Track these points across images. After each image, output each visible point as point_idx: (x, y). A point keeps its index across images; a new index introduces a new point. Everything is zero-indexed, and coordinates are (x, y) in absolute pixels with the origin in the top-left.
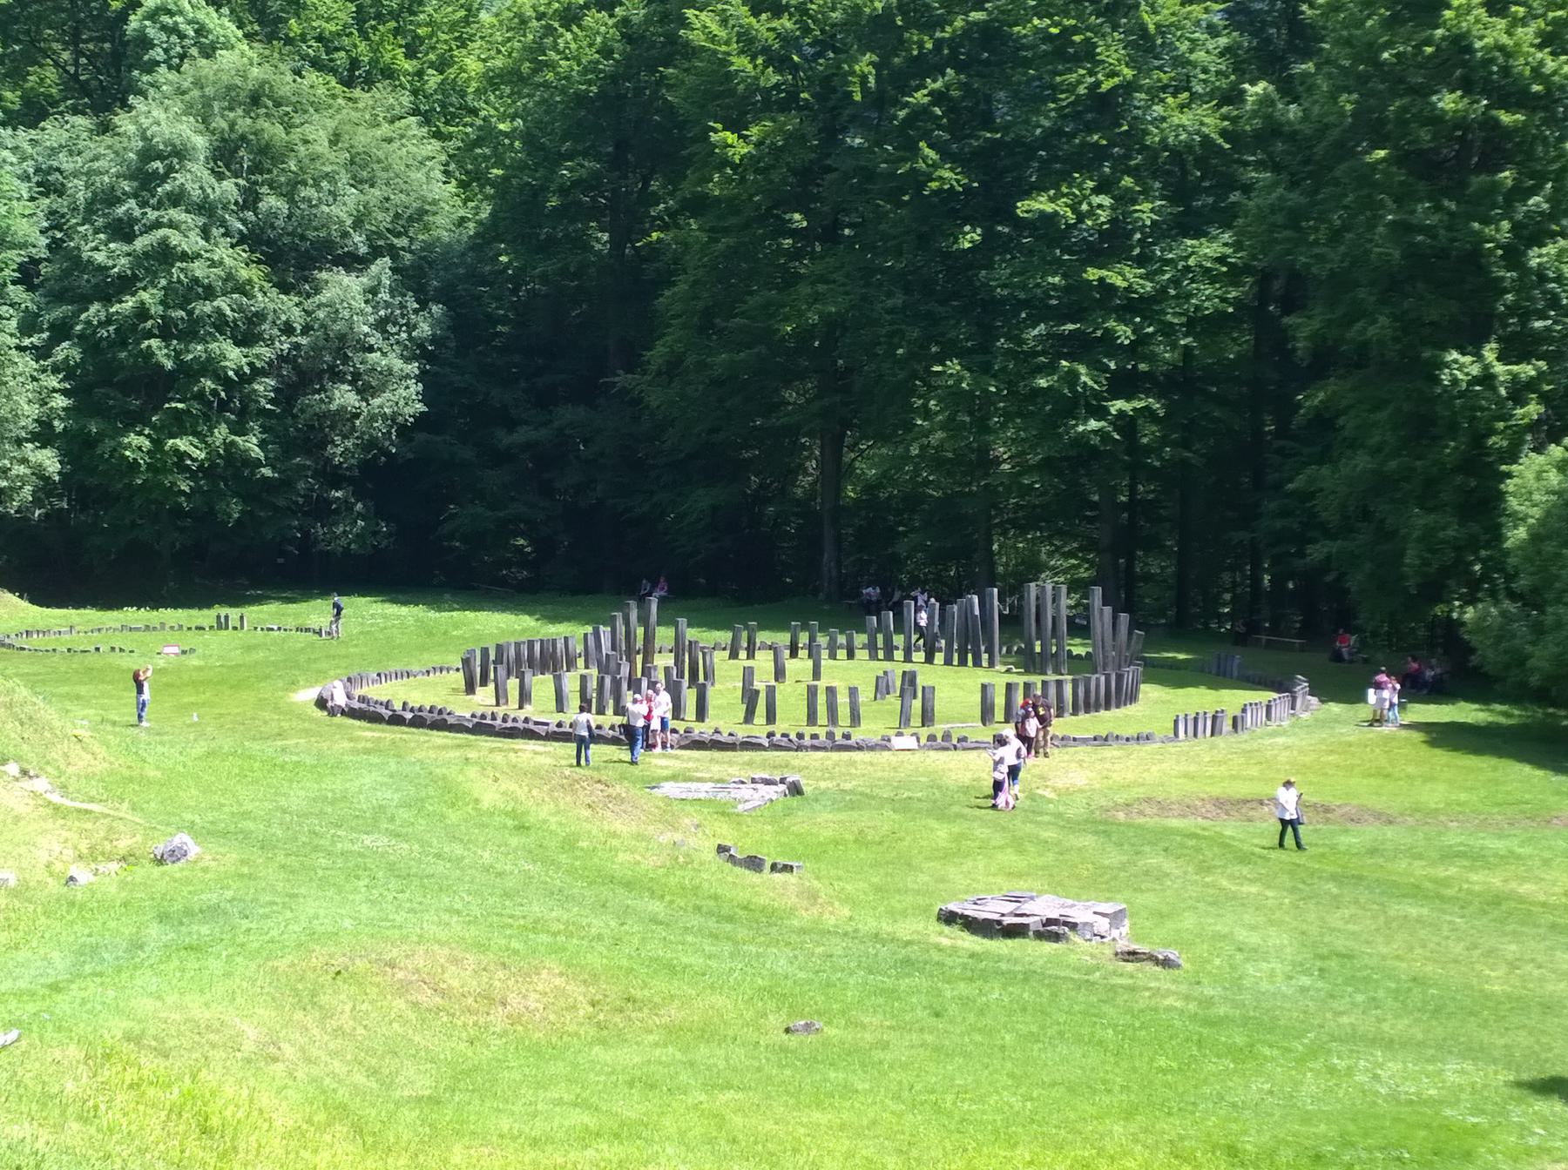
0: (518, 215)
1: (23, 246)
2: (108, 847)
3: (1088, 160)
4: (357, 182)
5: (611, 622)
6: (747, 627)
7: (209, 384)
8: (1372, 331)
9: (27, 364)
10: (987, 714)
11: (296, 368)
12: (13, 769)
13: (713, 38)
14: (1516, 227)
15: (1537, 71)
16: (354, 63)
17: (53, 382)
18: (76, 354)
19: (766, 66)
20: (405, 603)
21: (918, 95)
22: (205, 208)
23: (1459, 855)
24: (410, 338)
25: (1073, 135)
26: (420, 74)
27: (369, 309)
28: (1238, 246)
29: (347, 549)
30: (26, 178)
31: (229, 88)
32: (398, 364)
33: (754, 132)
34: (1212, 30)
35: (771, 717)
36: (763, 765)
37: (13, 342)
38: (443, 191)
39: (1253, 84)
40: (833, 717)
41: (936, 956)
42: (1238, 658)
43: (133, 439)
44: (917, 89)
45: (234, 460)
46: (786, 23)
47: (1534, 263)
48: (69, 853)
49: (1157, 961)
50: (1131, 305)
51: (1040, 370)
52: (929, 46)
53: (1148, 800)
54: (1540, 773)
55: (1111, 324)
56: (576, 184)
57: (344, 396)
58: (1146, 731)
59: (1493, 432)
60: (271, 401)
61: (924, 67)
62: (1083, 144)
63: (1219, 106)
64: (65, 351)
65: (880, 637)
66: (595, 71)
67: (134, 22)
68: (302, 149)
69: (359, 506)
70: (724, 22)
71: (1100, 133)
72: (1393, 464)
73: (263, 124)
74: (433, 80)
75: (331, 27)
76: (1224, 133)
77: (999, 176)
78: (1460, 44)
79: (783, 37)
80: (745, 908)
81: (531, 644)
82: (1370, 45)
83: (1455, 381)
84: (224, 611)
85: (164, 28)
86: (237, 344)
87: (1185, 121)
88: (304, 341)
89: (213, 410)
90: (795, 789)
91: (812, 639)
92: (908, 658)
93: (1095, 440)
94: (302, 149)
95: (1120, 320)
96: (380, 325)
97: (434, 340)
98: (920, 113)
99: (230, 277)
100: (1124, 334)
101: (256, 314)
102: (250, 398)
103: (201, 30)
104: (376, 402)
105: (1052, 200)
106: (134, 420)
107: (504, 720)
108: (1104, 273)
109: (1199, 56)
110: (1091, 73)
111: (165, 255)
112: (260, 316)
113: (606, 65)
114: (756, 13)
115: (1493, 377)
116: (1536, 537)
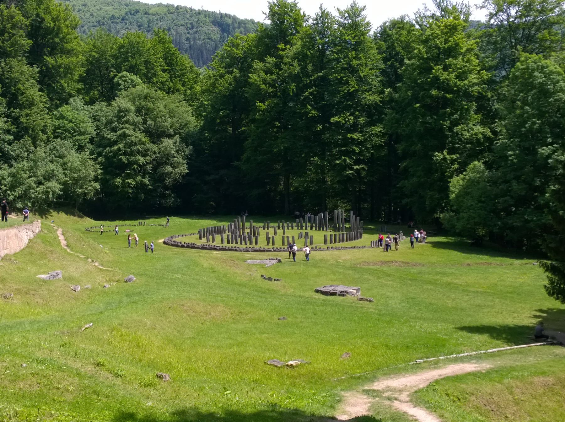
0: (210, 124)
1: (90, 134)
2: (113, 278)
3: (347, 108)
4: (171, 117)
5: (234, 222)
7: (136, 166)
8: (416, 148)
9: (91, 162)
10: (325, 242)
12: (90, 260)
13: (256, 81)
14: (451, 122)
15: (455, 85)
17: (98, 167)
18: (103, 160)
19: (269, 87)
20: (184, 218)
22: (134, 124)
23: (440, 273)
25: (343, 102)
26: (185, 90)
28: (384, 128)
30: (91, 117)
31: (139, 95)
32: (181, 161)
33: (267, 103)
34: (377, 76)
35: (273, 244)
36: (272, 255)
38: (192, 119)
41: (314, 300)
43: (118, 180)
45: (142, 184)
46: (274, 77)
47: (455, 131)
48: (104, 280)
49: (368, 301)
50: (359, 143)
51: (337, 159)
52: (309, 81)
53: (365, 262)
54: (459, 253)
55: (354, 147)
56: (224, 116)
57: (169, 169)
58: (364, 245)
59: (447, 172)
61: (308, 86)
62: (346, 104)
64: (101, 159)
65: (299, 224)
67: (116, 79)
70: (259, 77)
72: (422, 180)
74: (189, 92)
76: (380, 101)
77: (326, 112)
78: (437, 78)
81: (215, 227)
82: (415, 79)
83: (437, 159)
84: (140, 221)
85: (123, 81)
86: (142, 157)
87: (372, 98)
88: (159, 155)
89: (137, 173)
90: (280, 261)
91: (283, 225)
92: (306, 229)
95: (356, 146)
97: (190, 155)
99: (140, 140)
100: (357, 150)
102: (146, 169)
103: (132, 81)
104: (176, 170)
105: (339, 118)
106: (117, 176)
109: (374, 82)
110: (348, 87)
111: (124, 135)
112: (148, 150)
113: (231, 88)
114: (266, 74)
115: (446, 158)
116: (457, 197)
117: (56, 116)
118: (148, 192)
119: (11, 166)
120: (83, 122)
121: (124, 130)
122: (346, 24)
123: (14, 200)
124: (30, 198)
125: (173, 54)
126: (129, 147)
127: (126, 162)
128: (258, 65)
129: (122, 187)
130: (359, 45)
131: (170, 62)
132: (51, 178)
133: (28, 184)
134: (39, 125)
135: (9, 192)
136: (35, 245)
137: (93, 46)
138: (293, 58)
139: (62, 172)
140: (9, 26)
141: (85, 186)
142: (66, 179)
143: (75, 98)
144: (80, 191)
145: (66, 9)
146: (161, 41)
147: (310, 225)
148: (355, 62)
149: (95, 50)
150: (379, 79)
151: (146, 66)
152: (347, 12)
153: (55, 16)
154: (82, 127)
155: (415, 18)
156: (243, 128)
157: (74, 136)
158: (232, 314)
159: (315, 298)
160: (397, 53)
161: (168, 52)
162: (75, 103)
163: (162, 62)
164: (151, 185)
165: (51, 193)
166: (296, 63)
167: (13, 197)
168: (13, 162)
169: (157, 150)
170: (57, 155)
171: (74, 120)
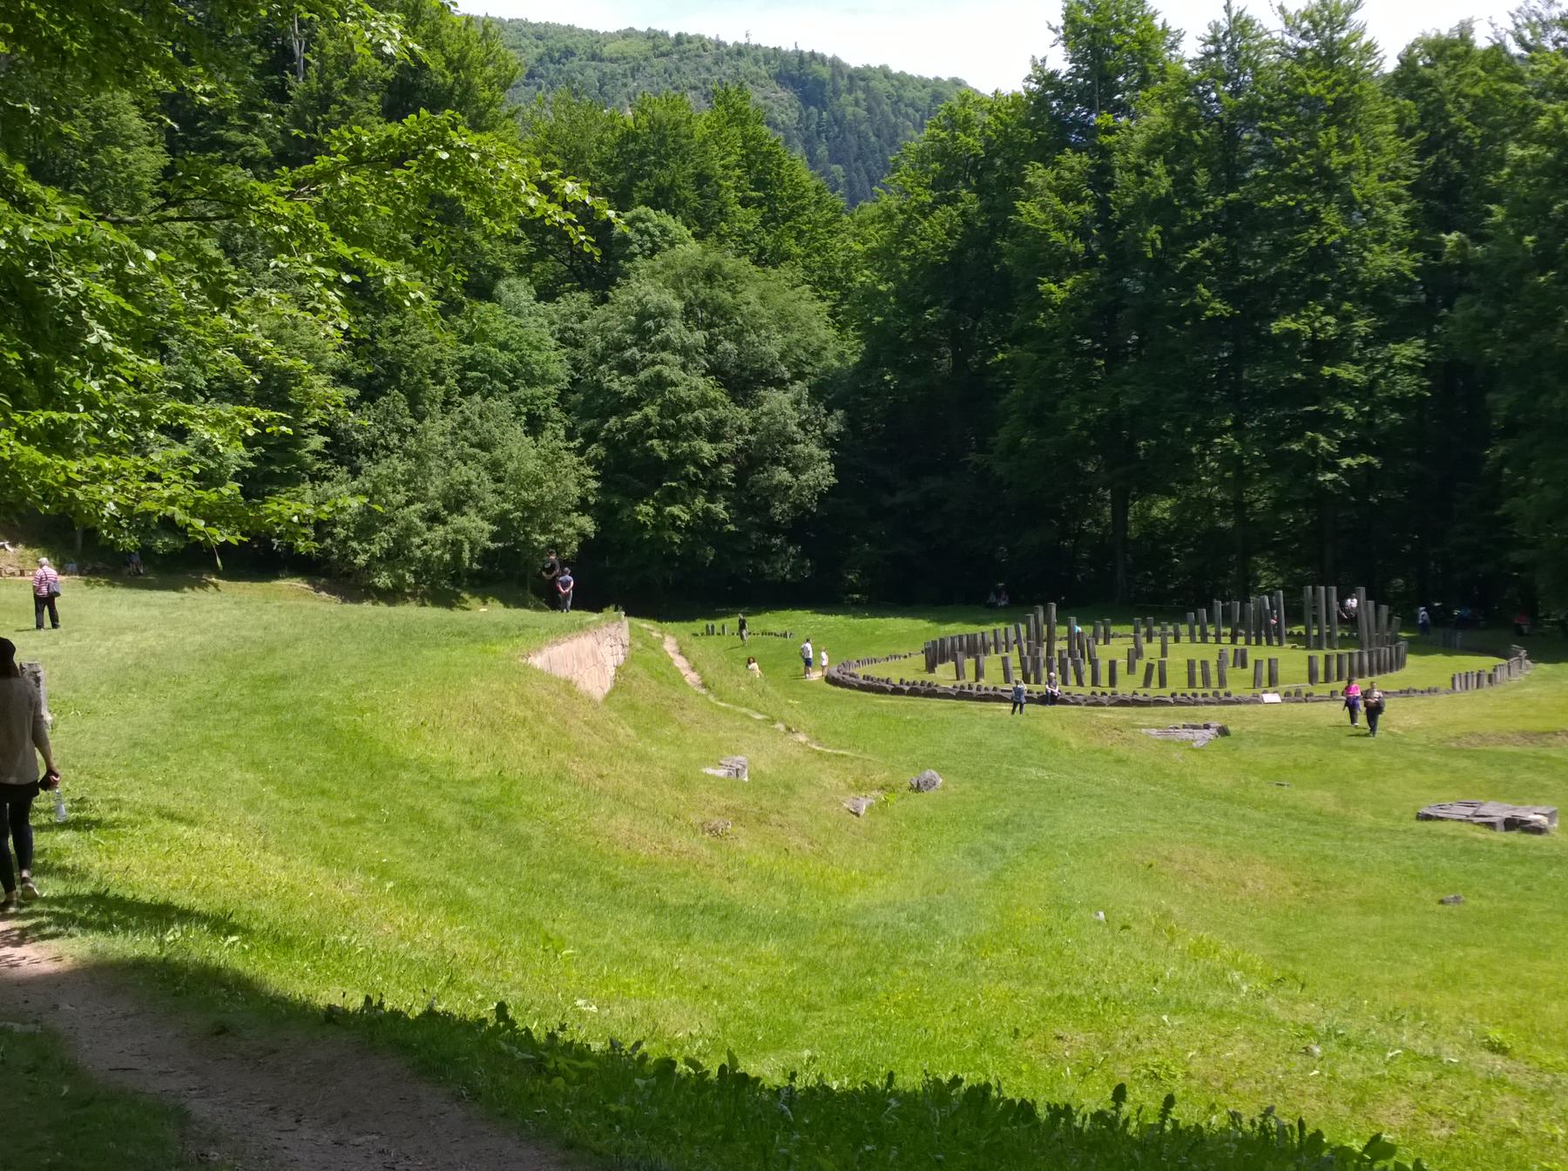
0: (883, 347)
1: (557, 381)
3: (1318, 290)
5: (1026, 621)
6: (1104, 623)
7: (692, 469)
9: (571, 459)
10: (1312, 677)
12: (780, 726)
13: (1035, 220)
16: (762, 251)
17: (588, 471)
18: (602, 452)
19: (1074, 237)
21: (1193, 252)
22: (685, 351)
25: (1304, 276)
26: (808, 256)
27: (796, 414)
28: (1427, 347)
29: (783, 578)
30: (552, 335)
32: (815, 451)
33: (1069, 283)
35: (1162, 683)
36: (1177, 716)
37: (561, 445)
38: (824, 332)
39: (1448, 233)
40: (1206, 682)
41: (1476, 845)
42: (1459, 636)
43: (642, 508)
44: (1192, 248)
46: (1087, 208)
51: (1288, 439)
52: (1199, 218)
53: (1472, 734)
56: (933, 324)
57: (782, 475)
58: (1432, 684)
60: (732, 480)
61: (1199, 232)
62: (1313, 282)
63: (1409, 252)
64: (595, 450)
65: (1197, 628)
66: (945, 247)
68: (744, 307)
70: (1043, 208)
71: (1321, 276)
73: (717, 291)
77: (1255, 302)
79: (1082, 217)
80: (1320, 814)
84: (710, 623)
85: (638, 230)
86: (710, 441)
87: (1384, 261)
88: (753, 438)
89: (694, 484)
90: (1223, 731)
92: (1218, 641)
93: (1330, 487)
94: (744, 307)
96: (801, 425)
97: (839, 434)
98: (1193, 265)
100: (1350, 413)
101: (720, 421)
102: (720, 476)
103: (664, 231)
105: (1294, 320)
106: (639, 497)
107: (979, 689)
108: (1334, 370)
109: (1389, 217)
111: (660, 383)
112: (721, 423)
113: (952, 244)
114: (1065, 201)
117: (461, 332)
119: (355, 472)
121: (658, 367)
122: (1304, 50)
123: (368, 565)
124: (410, 561)
125: (770, 153)
126: (673, 416)
127: (665, 456)
128: (1037, 174)
129: (654, 526)
130: (1342, 111)
131: (761, 173)
132: (464, 502)
135: (354, 544)
137: (548, 137)
138: (1150, 152)
139: (490, 486)
140: (339, 84)
141: (555, 527)
142: (507, 506)
143: (512, 281)
144: (542, 538)
145: (485, 34)
146: (738, 117)
147: (1229, 630)
148: (1336, 160)
149: (554, 148)
150: (1404, 207)
151: (699, 187)
152: (1304, 16)
153: (456, 56)
154: (537, 362)
155: (1512, 27)
156: (1000, 356)
157: (514, 389)
158: (1296, 884)
159: (1476, 840)
160: (1454, 133)
161: (753, 151)
163: (739, 178)
165: (467, 546)
166: (1158, 168)
167: (365, 557)
168: (363, 461)
169: (746, 422)
170: (475, 439)
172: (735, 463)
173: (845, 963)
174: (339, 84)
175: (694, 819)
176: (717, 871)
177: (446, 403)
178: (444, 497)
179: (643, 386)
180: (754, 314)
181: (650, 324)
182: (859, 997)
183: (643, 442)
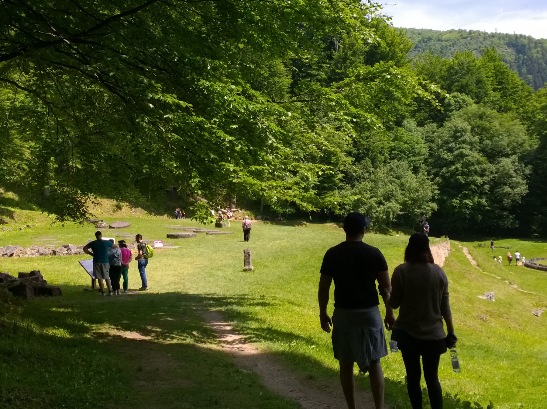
1: (424, 155)
2: (541, 303)
7: (473, 187)
9: (429, 183)
11: (495, 183)
12: (507, 282)
16: (501, 107)
17: (435, 187)
18: (440, 180)
22: (471, 143)
24: (524, 174)
26: (518, 109)
27: (513, 167)
29: (508, 227)
30: (422, 138)
32: (520, 180)
57: (508, 189)
60: (488, 191)
64: (438, 179)
68: (494, 128)
69: (511, 217)
75: (496, 99)
84: (480, 243)
86: (480, 177)
88: (496, 175)
89: (474, 192)
94: (494, 128)
96: (515, 171)
97: (530, 174)
101: (484, 169)
103: (464, 101)
104: (516, 190)
106: (454, 196)
111: (462, 155)
112: (484, 170)
118: (485, 213)
119: (353, 187)
120: (417, 143)
121: (461, 150)
124: (372, 218)
125: (504, 72)
126: (466, 168)
127: (463, 182)
129: (459, 207)
133: (369, 204)
134: (377, 147)
136: (452, 264)
137: (422, 69)
140: (350, 53)
141: (423, 207)
142: (406, 199)
143: (409, 120)
144: (418, 211)
145: (400, 34)
146: (492, 59)
149: (425, 72)
153: (390, 42)
161: (498, 71)
162: (408, 125)
163: (492, 81)
164: (489, 206)
165: (391, 213)
168: (356, 183)
170: (395, 175)
171: (408, 142)
172: (490, 184)
173: (533, 372)
174: (350, 53)
175: (474, 314)
176: (484, 334)
177: (385, 162)
178: (384, 196)
179: (455, 157)
180: (497, 130)
181: (459, 134)
182: (539, 384)
183: (456, 177)
